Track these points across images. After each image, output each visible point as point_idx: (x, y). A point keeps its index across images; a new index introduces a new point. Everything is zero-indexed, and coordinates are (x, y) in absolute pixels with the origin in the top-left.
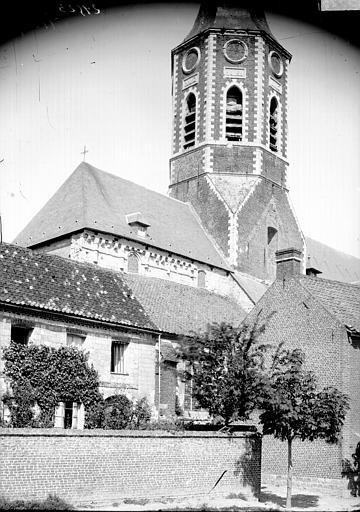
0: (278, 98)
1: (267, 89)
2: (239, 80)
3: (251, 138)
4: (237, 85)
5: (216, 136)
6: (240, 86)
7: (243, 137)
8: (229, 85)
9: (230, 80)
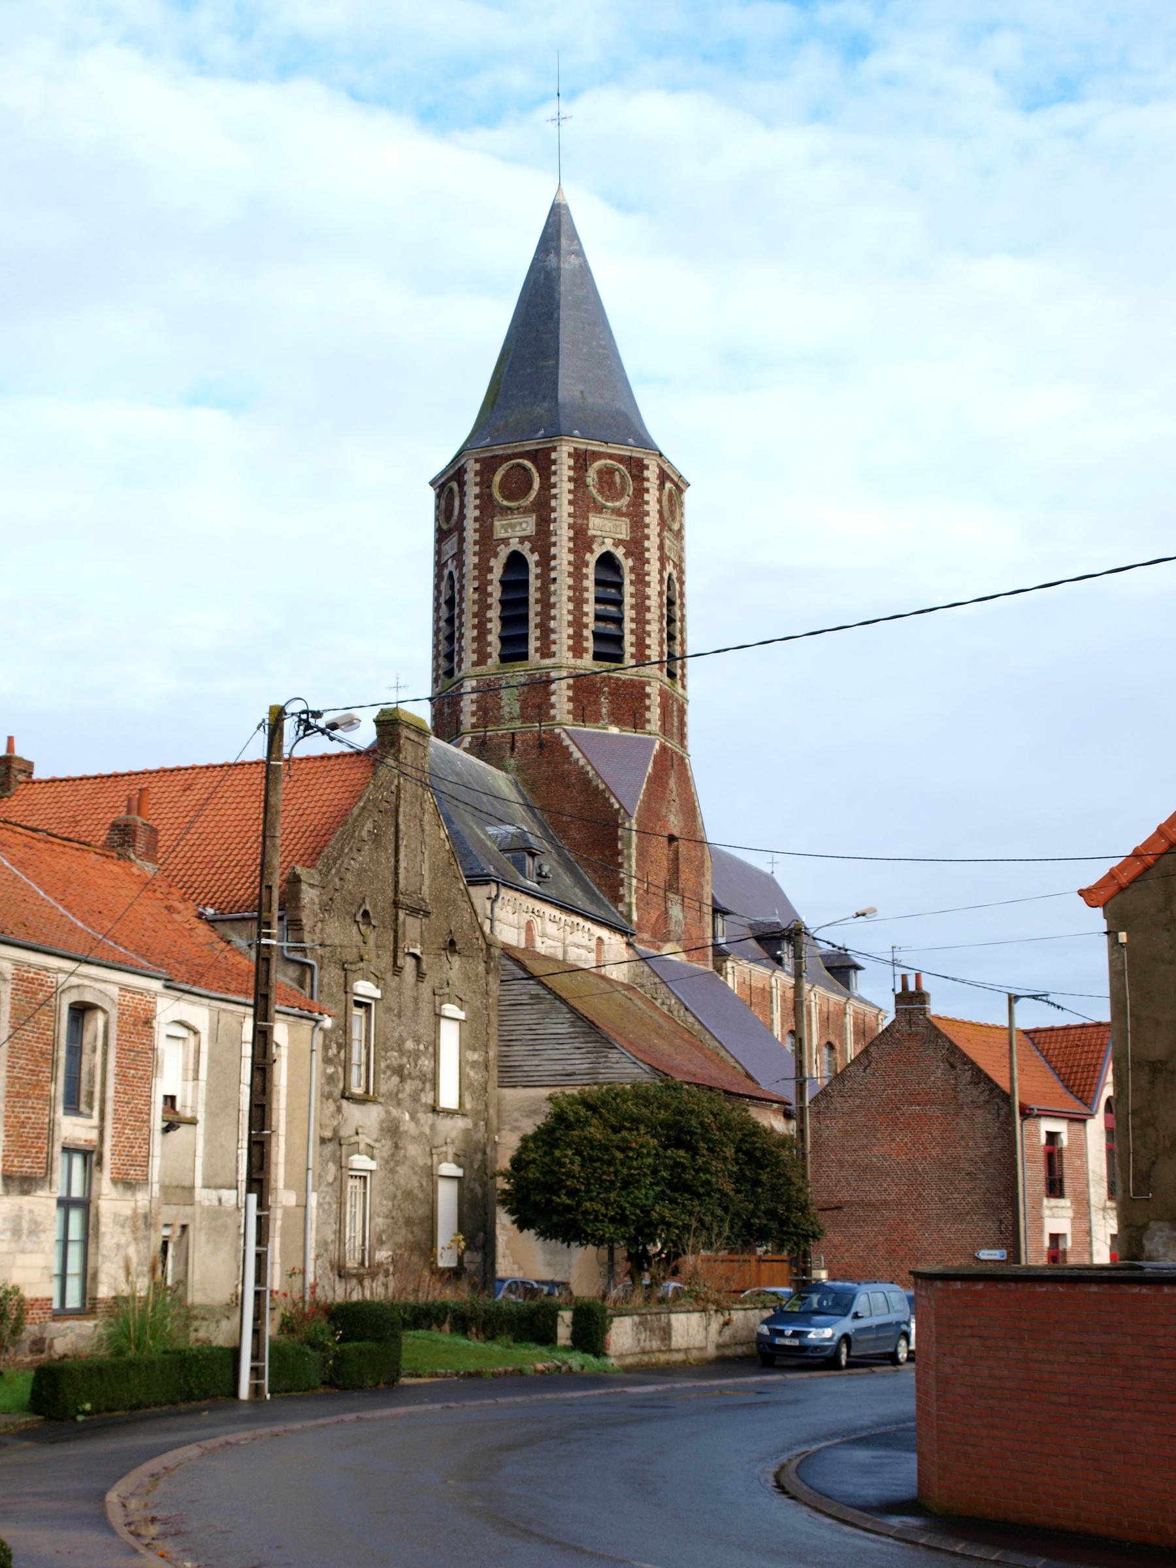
2: (618, 543)
4: (612, 549)
6: (619, 553)
7: (627, 656)
8: (599, 551)
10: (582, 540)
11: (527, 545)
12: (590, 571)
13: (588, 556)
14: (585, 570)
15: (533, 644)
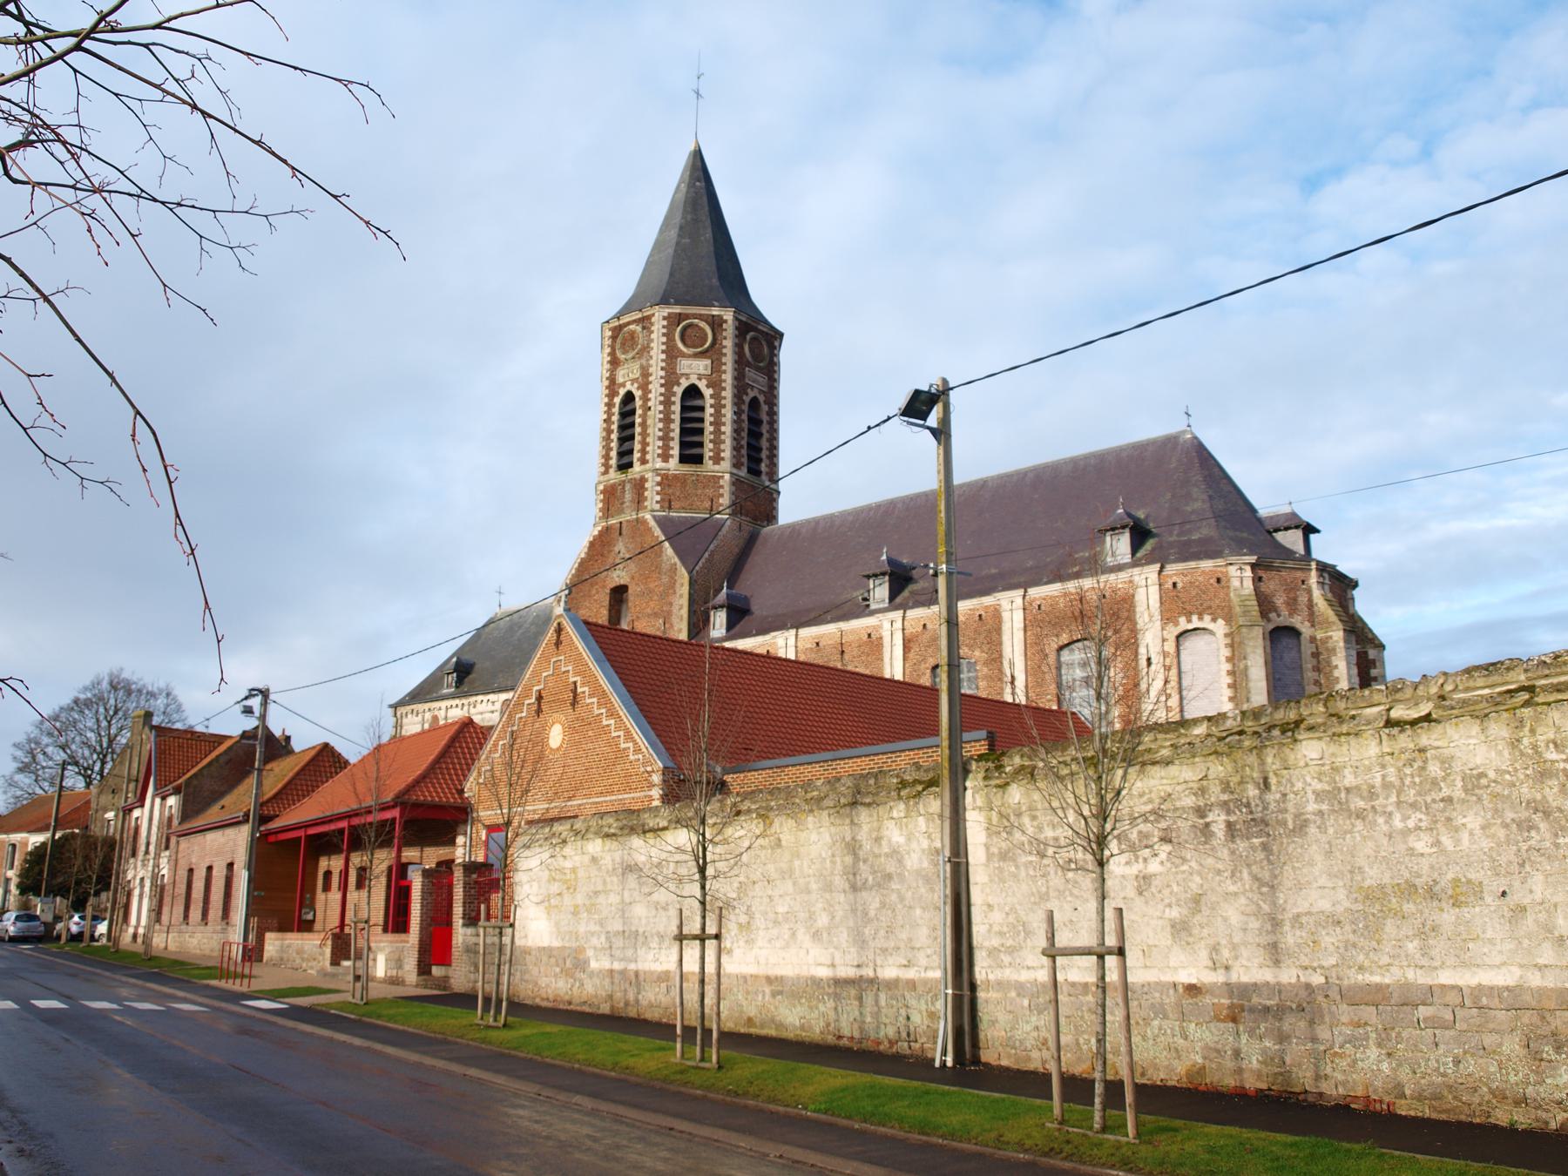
0: (761, 398)
1: (741, 388)
3: (717, 459)
5: (665, 457)
6: (702, 385)
8: (685, 383)
9: (687, 376)
10: (671, 379)
11: (636, 385)
12: (677, 399)
13: (675, 389)
14: (673, 399)
15: (637, 455)
